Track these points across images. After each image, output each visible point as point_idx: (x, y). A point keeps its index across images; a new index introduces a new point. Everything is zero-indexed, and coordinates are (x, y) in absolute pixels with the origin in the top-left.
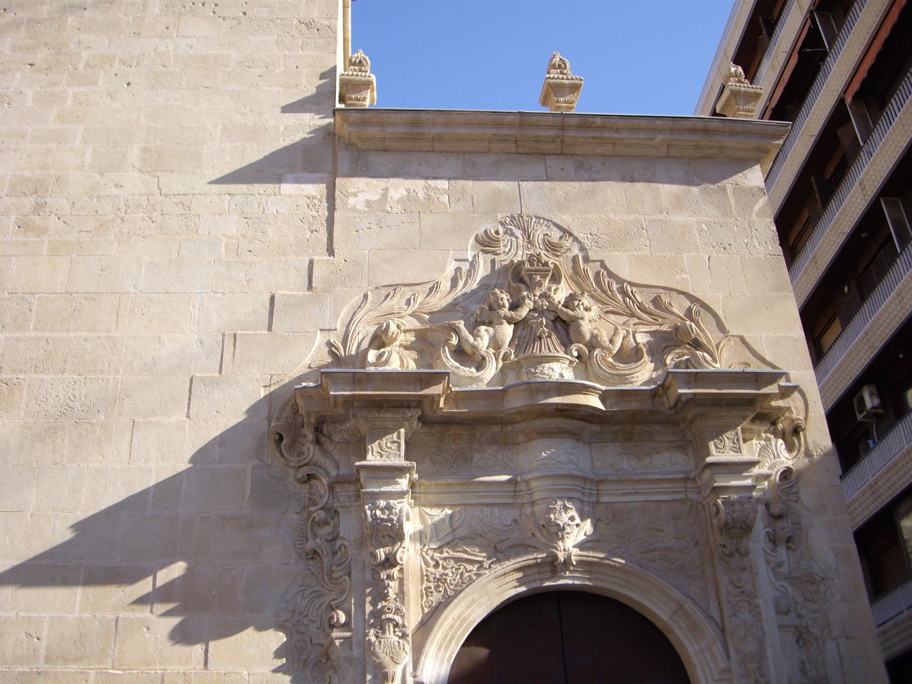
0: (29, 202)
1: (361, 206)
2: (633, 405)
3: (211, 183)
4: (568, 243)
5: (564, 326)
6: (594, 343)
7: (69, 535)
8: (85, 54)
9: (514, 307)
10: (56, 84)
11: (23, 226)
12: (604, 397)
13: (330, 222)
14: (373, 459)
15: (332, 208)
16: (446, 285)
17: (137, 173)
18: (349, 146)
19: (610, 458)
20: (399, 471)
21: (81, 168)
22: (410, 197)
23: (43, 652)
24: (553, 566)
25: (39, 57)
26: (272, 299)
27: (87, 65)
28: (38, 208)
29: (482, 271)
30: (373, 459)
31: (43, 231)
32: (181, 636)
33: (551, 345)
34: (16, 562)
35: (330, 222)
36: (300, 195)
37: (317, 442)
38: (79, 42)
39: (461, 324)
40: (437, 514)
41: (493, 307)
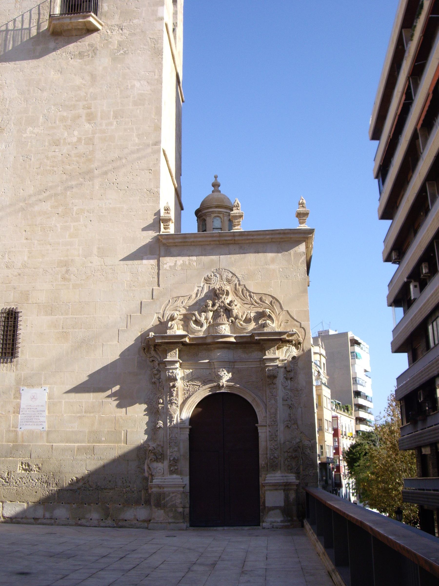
0: (64, 269)
1: (168, 268)
2: (244, 340)
3: (120, 261)
4: (234, 278)
5: (228, 312)
6: (236, 318)
7: (87, 379)
8: (75, 208)
9: (213, 305)
10: (67, 222)
11: (64, 278)
12: (235, 338)
13: (158, 274)
14: (169, 358)
15: (159, 269)
16: (194, 296)
17: (97, 257)
18: (164, 244)
19: (240, 354)
20: (176, 362)
21: (79, 256)
22: (184, 264)
23: (84, 410)
24: (219, 387)
25: (60, 210)
26: (141, 302)
28: (67, 271)
29: (206, 290)
30: (169, 358)
31: (69, 280)
32: (119, 406)
33: (223, 319)
34: (74, 386)
35: (158, 274)
36: (149, 264)
37: (155, 350)
38: (72, 203)
39: (196, 313)
40: (188, 371)
41: (207, 306)
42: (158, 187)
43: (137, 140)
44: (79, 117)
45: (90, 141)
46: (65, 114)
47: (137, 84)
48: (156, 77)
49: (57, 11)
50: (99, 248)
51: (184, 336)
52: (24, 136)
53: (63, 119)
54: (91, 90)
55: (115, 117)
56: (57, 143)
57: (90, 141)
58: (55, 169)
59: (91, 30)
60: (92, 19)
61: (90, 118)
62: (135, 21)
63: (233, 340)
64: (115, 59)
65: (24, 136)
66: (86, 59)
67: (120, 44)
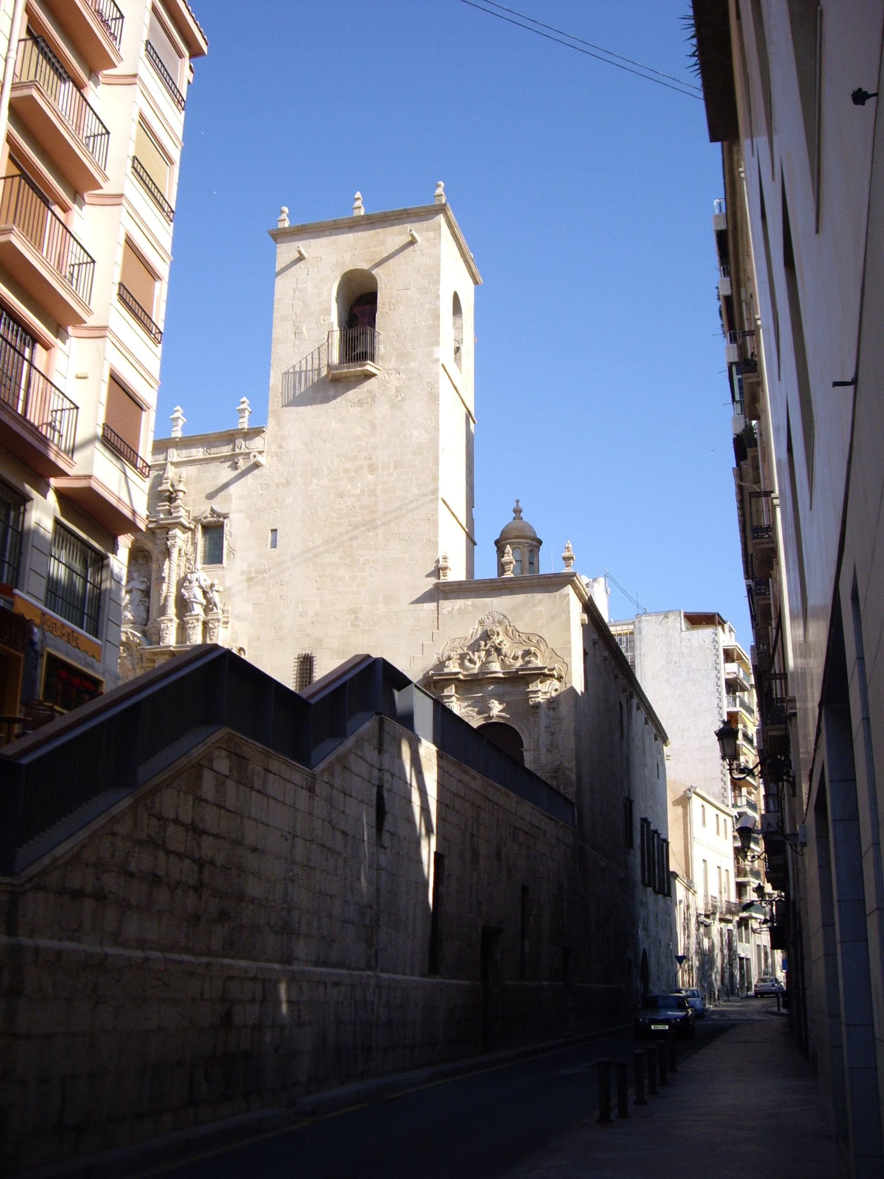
0: (353, 616)
2: (511, 675)
4: (505, 620)
5: (498, 651)
6: (505, 656)
8: (361, 559)
9: (485, 645)
11: (353, 625)
12: (503, 673)
14: (446, 693)
16: (469, 637)
18: (442, 591)
19: (508, 688)
20: (452, 696)
22: (460, 609)
24: (490, 717)
25: (348, 561)
27: (363, 564)
28: (356, 618)
29: (480, 632)
30: (446, 693)
31: (358, 626)
33: (494, 655)
39: (470, 653)
41: (480, 646)
42: (437, 536)
43: (416, 491)
44: (361, 468)
46: (348, 466)
48: (434, 424)
49: (335, 358)
50: (384, 596)
51: (458, 673)
52: (311, 488)
53: (346, 471)
54: (372, 440)
55: (396, 468)
56: (341, 495)
57: (372, 493)
58: (341, 521)
59: (369, 376)
60: (369, 367)
61: (372, 469)
62: (412, 364)
63: (501, 675)
64: (394, 406)
65: (311, 488)
66: (366, 406)
67: (398, 390)
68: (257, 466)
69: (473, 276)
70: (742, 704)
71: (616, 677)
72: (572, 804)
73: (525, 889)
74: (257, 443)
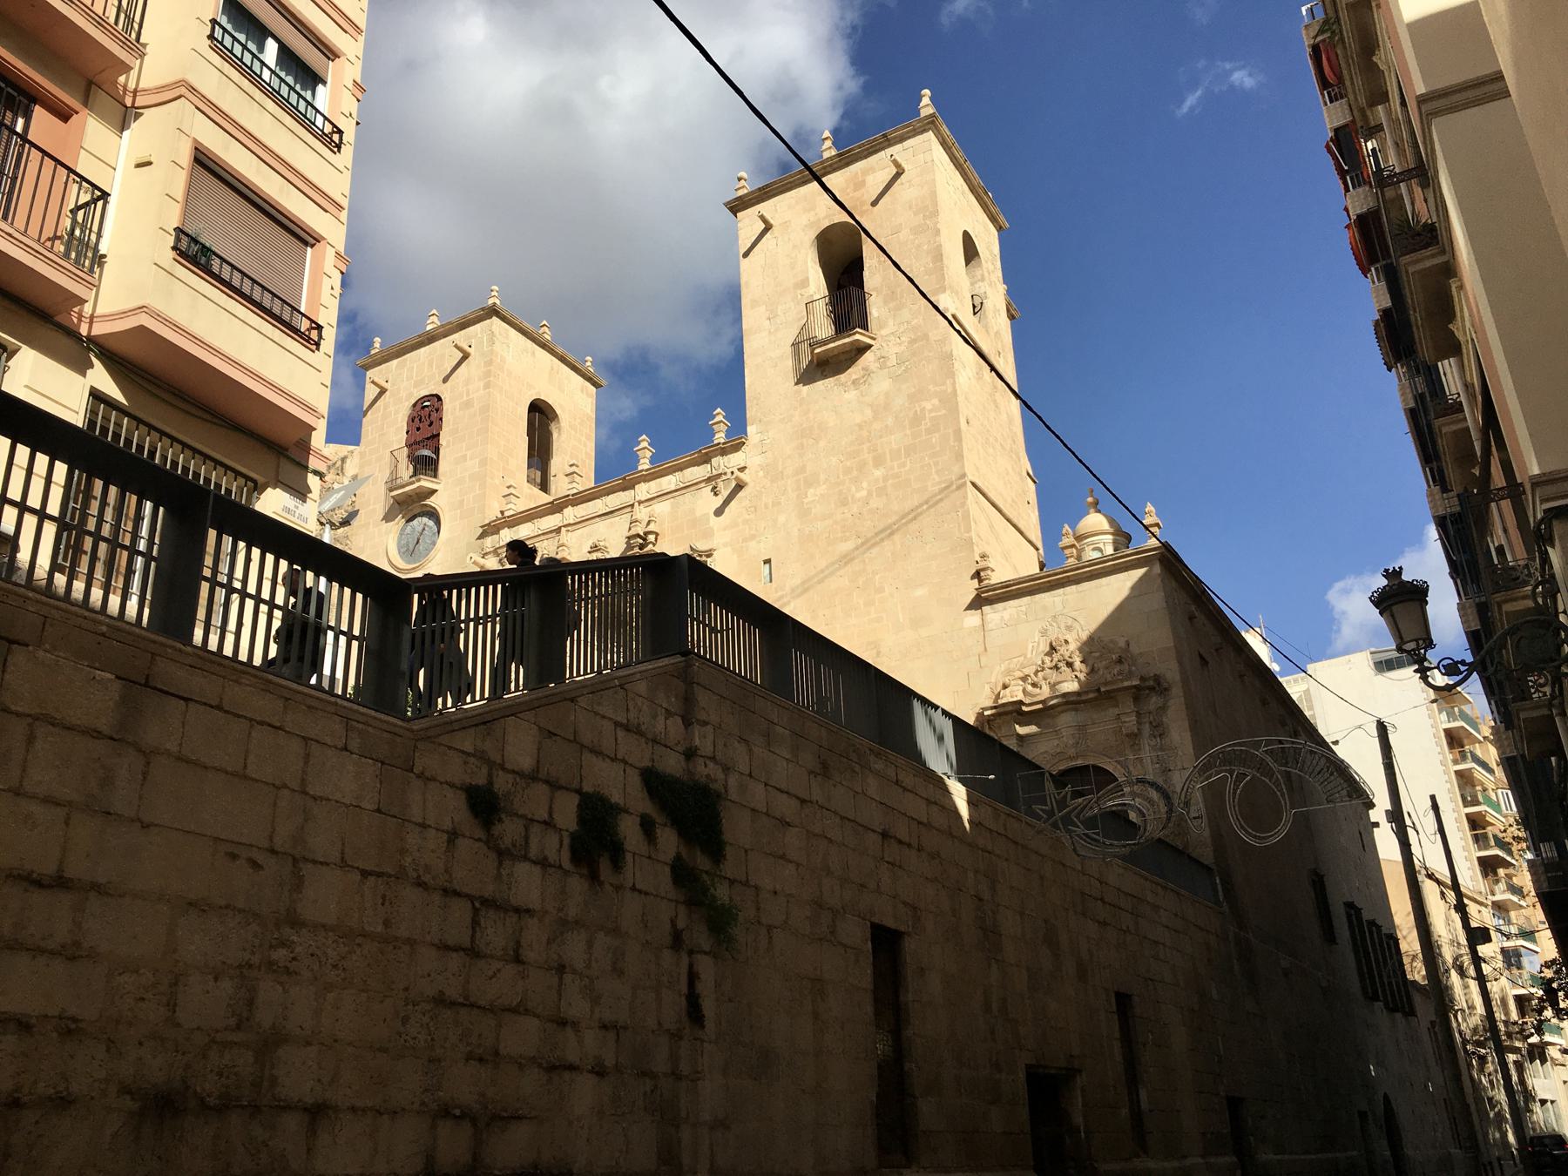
4: (1076, 625)
43: (937, 479)
45: (882, 491)
47: (928, 406)
53: (848, 471)
56: (844, 502)
59: (862, 349)
60: (859, 336)
61: (878, 462)
66: (863, 388)
68: (740, 487)
69: (993, 219)
70: (1463, 716)
71: (1264, 703)
72: (1208, 869)
73: (1123, 1001)
74: (735, 459)
